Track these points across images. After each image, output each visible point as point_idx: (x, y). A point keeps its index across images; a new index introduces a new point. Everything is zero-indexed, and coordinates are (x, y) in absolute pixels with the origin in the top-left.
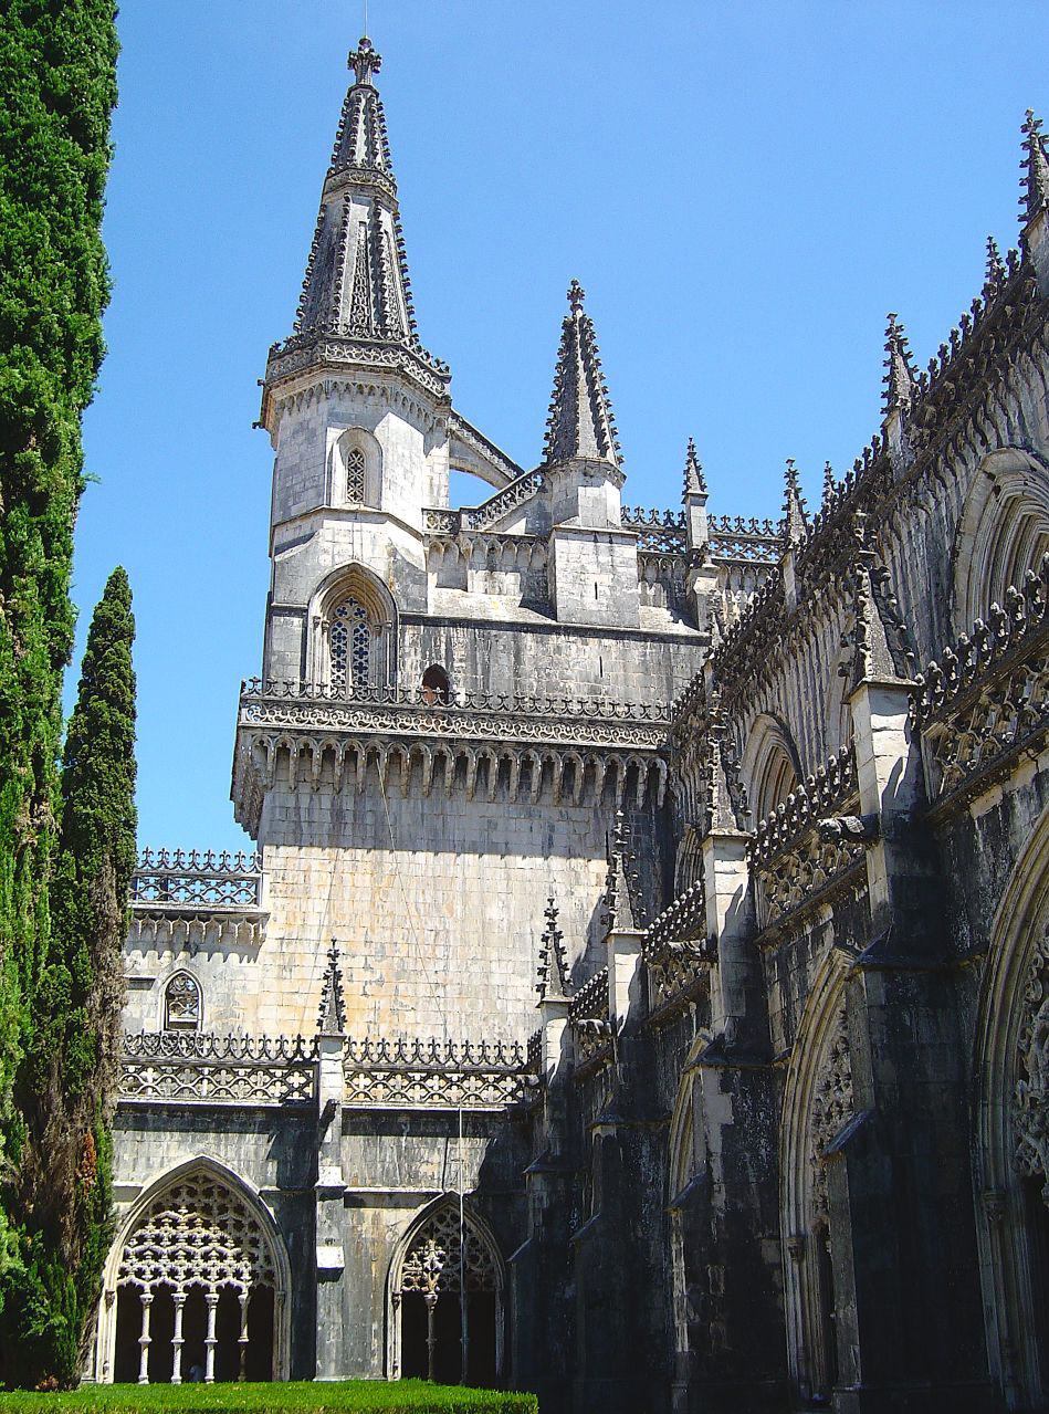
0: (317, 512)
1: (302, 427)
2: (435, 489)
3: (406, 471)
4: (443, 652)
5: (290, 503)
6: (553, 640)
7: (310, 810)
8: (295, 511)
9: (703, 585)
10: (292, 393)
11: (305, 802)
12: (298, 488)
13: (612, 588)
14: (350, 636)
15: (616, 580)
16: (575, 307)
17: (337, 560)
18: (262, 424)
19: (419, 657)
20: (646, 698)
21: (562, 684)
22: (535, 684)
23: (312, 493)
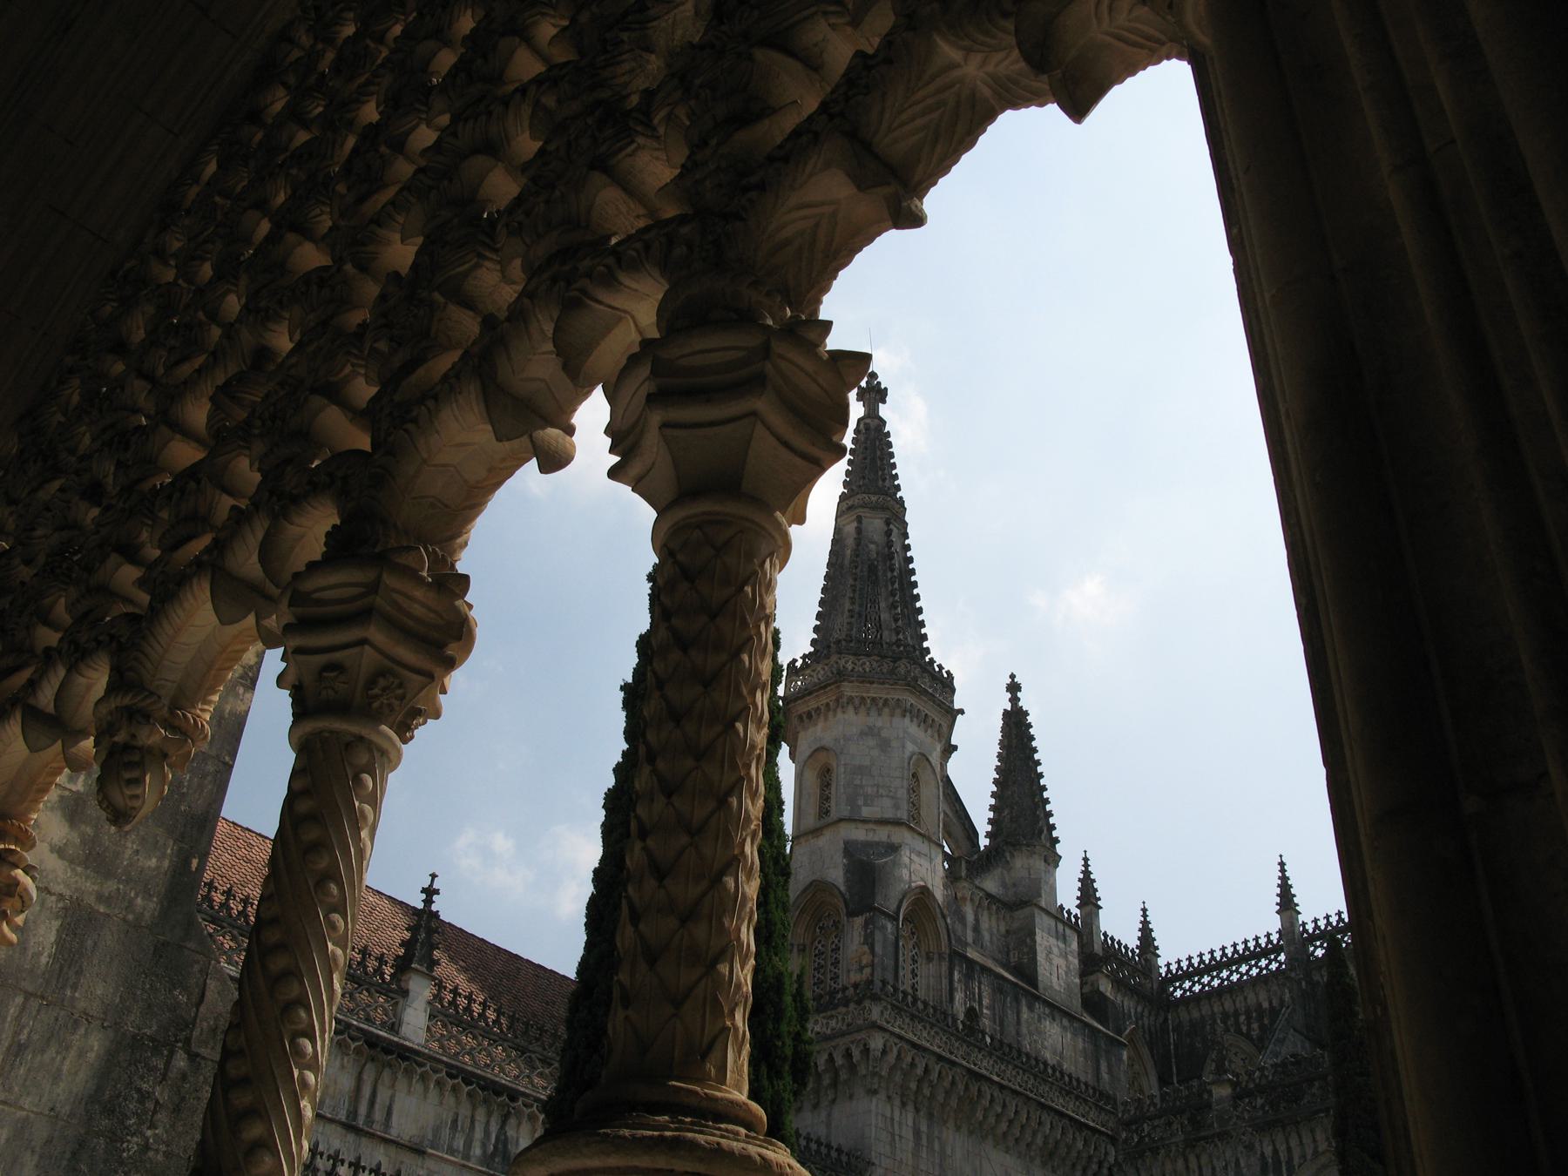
0: (897, 823)
1: (869, 732)
5: (860, 802)
7: (900, 1124)
8: (866, 812)
9: (1106, 987)
11: (897, 1119)
12: (869, 790)
16: (1014, 700)
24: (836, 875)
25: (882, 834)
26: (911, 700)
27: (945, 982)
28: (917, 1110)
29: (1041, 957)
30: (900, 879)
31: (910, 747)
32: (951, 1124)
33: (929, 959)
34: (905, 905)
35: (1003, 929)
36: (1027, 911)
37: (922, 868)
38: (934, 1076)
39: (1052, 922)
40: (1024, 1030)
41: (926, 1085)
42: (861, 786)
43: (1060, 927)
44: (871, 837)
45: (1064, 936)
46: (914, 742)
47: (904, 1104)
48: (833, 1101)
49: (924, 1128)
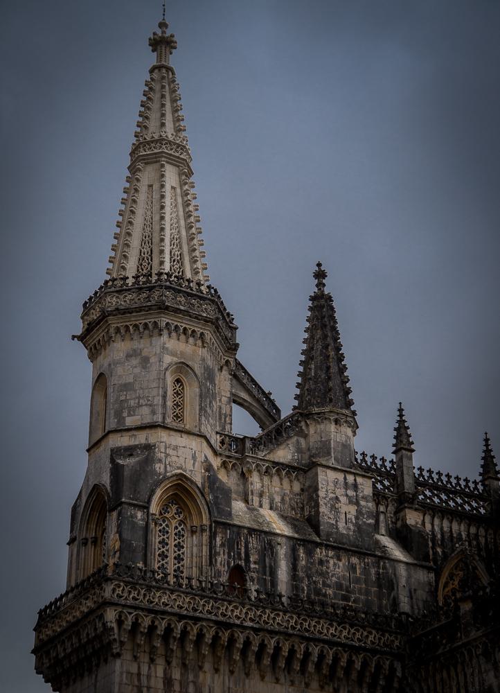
0: (153, 426)
2: (223, 417)
3: (211, 402)
4: (243, 555)
5: (125, 414)
6: (319, 553)
7: (149, 677)
8: (130, 421)
10: (128, 324)
12: (132, 403)
13: (357, 518)
14: (172, 531)
15: (359, 512)
16: (320, 285)
17: (168, 468)
18: (81, 338)
19: (226, 557)
20: (380, 607)
21: (324, 591)
22: (305, 588)
23: (145, 411)
24: (106, 479)
25: (141, 438)
26: (164, 320)
27: (205, 550)
28: (169, 663)
29: (323, 509)
30: (154, 472)
31: (168, 359)
32: (208, 666)
33: (193, 532)
34: (159, 492)
35: (297, 487)
36: (313, 470)
37: (185, 455)
38: (177, 633)
39: (340, 476)
40: (301, 574)
41: (171, 641)
42: (126, 401)
43: (350, 478)
44: (133, 442)
45: (355, 486)
46: (173, 354)
47: (152, 660)
48: (98, 665)
49: (176, 675)
